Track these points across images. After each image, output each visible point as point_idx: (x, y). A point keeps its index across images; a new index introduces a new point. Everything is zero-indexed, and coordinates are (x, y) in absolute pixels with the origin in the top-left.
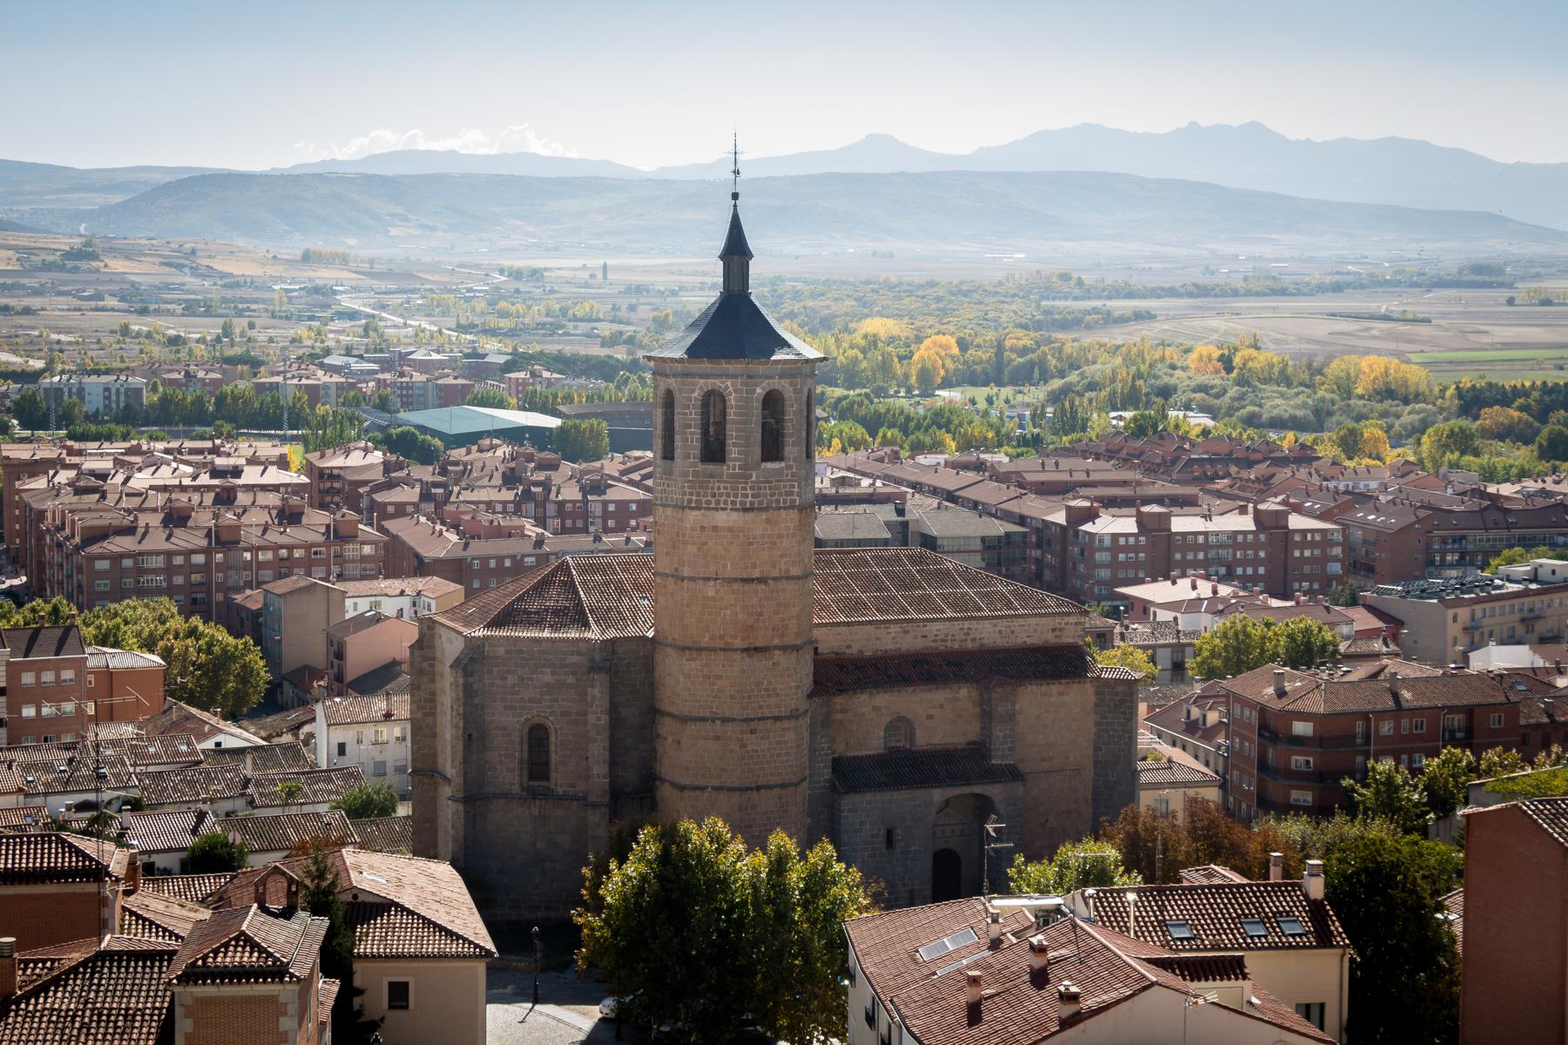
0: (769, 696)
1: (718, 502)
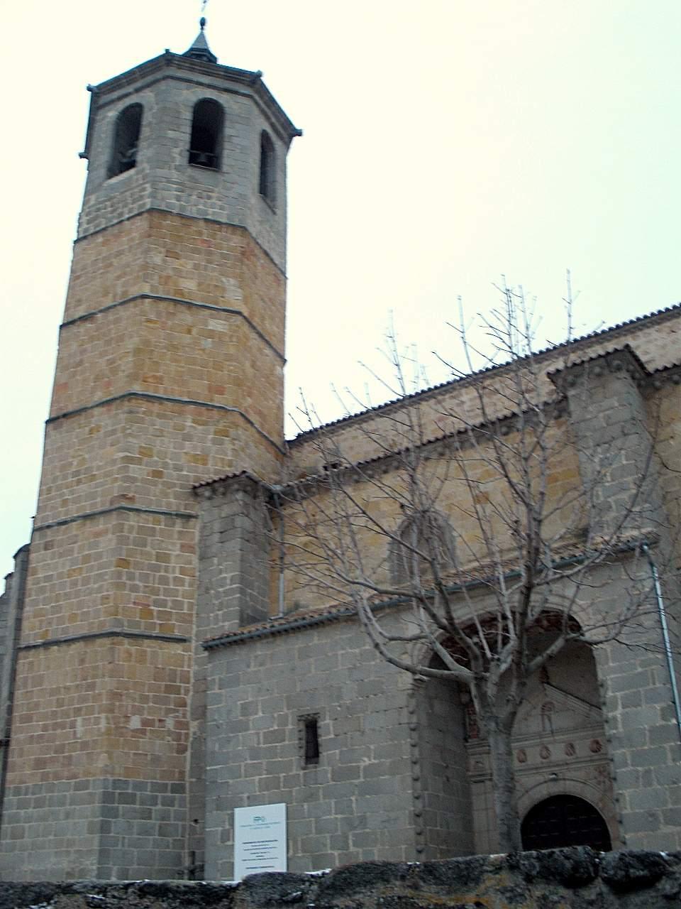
0: (79, 482)
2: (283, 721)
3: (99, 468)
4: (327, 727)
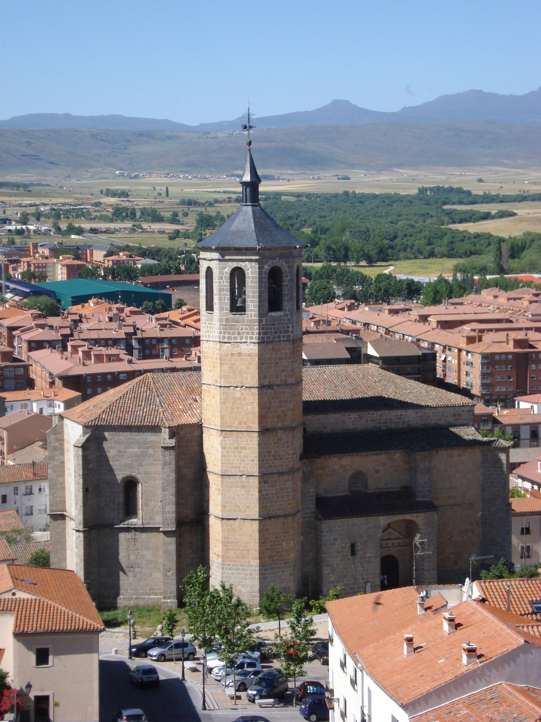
0: (275, 459)
1: (241, 338)
2: (346, 543)
3: (283, 455)
4: (359, 546)
